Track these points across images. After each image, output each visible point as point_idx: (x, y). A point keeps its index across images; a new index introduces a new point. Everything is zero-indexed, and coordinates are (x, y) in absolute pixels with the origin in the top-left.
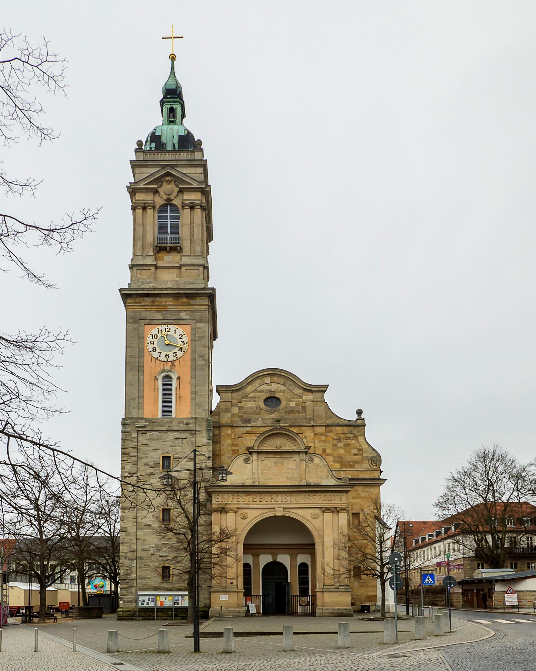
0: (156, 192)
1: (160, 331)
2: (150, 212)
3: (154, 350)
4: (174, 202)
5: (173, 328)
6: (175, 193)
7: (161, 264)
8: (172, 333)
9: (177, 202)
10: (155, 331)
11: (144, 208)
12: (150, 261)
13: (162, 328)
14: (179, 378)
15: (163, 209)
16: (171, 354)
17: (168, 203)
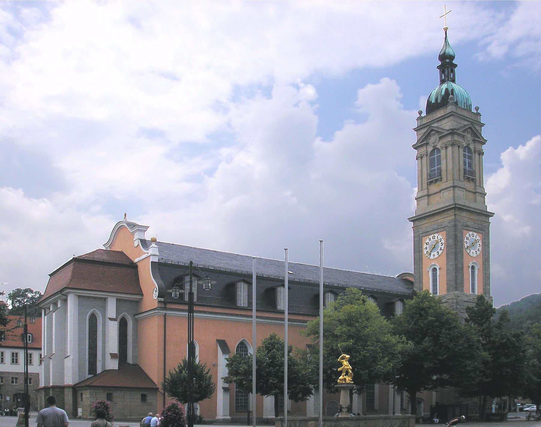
0: (427, 144)
1: (430, 240)
2: (424, 159)
3: (427, 252)
4: (437, 147)
5: (436, 235)
6: (437, 142)
7: (431, 192)
8: (436, 237)
9: (438, 146)
10: (427, 241)
11: (421, 158)
12: (425, 192)
13: (431, 237)
14: (440, 269)
15: (432, 152)
16: (436, 253)
17: (435, 148)
